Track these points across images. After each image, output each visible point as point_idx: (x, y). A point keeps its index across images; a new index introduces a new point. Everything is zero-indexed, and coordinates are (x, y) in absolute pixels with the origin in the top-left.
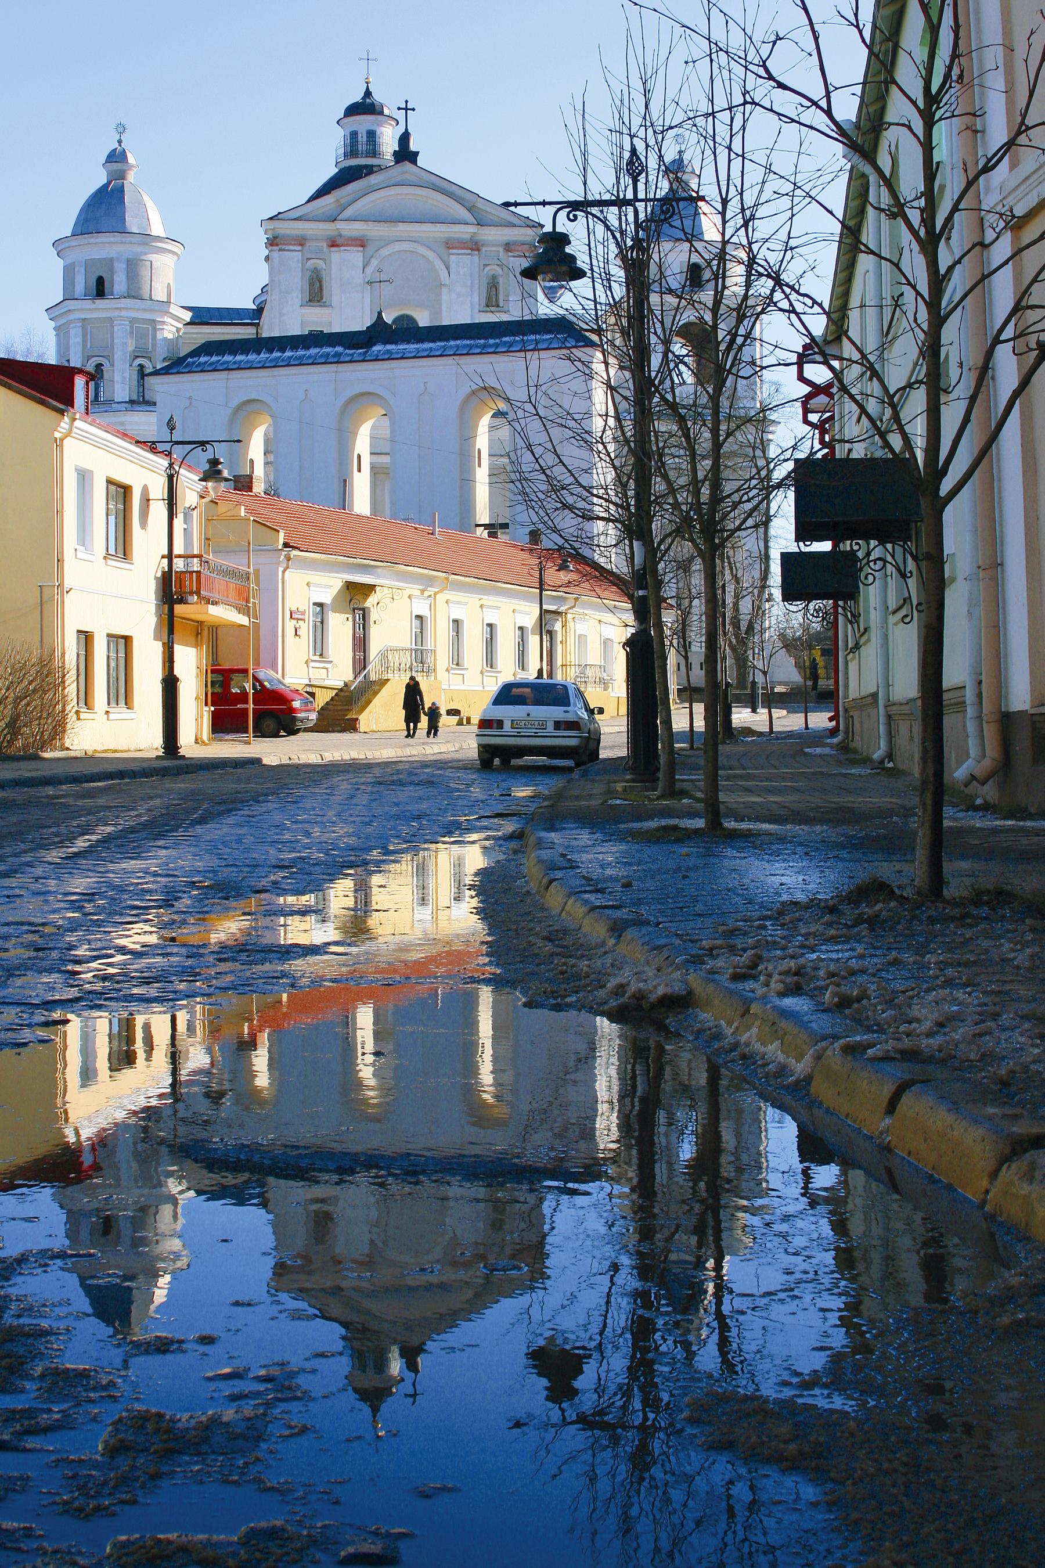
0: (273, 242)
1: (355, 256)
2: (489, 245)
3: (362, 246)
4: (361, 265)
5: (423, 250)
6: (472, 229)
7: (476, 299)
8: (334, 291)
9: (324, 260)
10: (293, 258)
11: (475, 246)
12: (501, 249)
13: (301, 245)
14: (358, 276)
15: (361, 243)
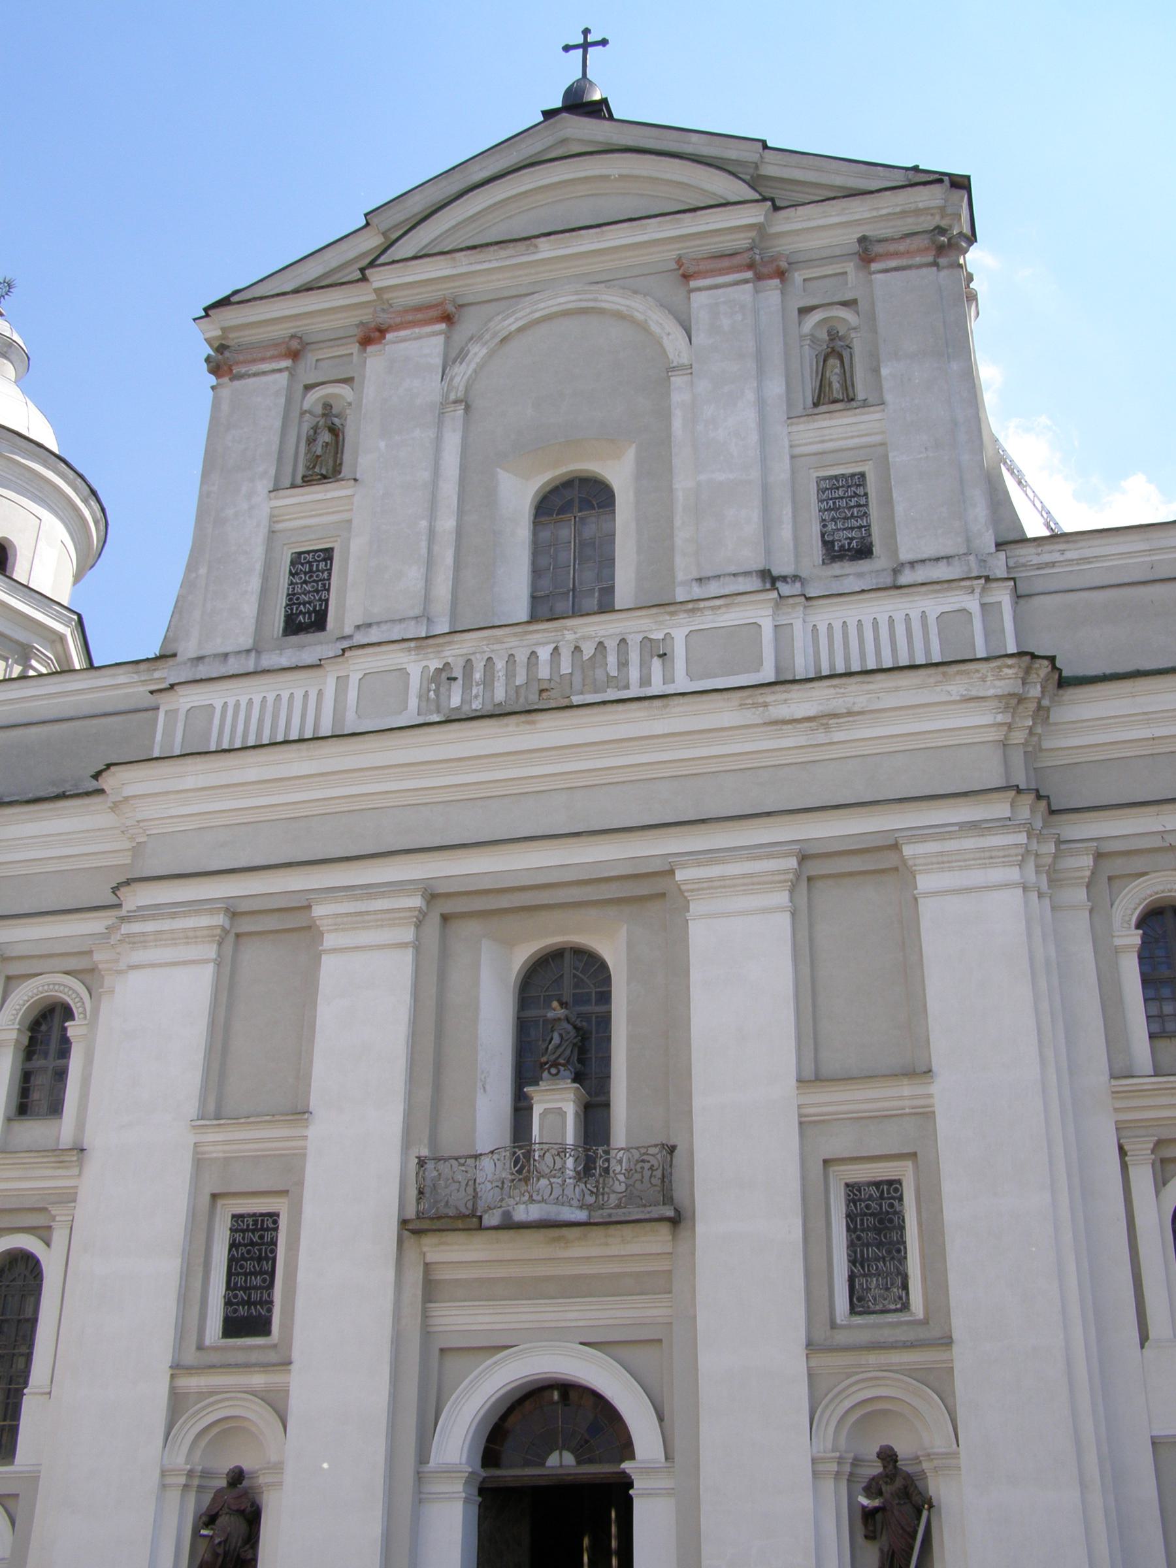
0: (222, 364)
1: (424, 347)
2: (809, 263)
3: (448, 318)
4: (438, 361)
5: (612, 300)
6: (754, 215)
7: (776, 387)
8: (367, 449)
9: (348, 381)
10: (267, 391)
11: (763, 265)
12: (850, 267)
13: (295, 355)
14: (429, 389)
15: (447, 316)
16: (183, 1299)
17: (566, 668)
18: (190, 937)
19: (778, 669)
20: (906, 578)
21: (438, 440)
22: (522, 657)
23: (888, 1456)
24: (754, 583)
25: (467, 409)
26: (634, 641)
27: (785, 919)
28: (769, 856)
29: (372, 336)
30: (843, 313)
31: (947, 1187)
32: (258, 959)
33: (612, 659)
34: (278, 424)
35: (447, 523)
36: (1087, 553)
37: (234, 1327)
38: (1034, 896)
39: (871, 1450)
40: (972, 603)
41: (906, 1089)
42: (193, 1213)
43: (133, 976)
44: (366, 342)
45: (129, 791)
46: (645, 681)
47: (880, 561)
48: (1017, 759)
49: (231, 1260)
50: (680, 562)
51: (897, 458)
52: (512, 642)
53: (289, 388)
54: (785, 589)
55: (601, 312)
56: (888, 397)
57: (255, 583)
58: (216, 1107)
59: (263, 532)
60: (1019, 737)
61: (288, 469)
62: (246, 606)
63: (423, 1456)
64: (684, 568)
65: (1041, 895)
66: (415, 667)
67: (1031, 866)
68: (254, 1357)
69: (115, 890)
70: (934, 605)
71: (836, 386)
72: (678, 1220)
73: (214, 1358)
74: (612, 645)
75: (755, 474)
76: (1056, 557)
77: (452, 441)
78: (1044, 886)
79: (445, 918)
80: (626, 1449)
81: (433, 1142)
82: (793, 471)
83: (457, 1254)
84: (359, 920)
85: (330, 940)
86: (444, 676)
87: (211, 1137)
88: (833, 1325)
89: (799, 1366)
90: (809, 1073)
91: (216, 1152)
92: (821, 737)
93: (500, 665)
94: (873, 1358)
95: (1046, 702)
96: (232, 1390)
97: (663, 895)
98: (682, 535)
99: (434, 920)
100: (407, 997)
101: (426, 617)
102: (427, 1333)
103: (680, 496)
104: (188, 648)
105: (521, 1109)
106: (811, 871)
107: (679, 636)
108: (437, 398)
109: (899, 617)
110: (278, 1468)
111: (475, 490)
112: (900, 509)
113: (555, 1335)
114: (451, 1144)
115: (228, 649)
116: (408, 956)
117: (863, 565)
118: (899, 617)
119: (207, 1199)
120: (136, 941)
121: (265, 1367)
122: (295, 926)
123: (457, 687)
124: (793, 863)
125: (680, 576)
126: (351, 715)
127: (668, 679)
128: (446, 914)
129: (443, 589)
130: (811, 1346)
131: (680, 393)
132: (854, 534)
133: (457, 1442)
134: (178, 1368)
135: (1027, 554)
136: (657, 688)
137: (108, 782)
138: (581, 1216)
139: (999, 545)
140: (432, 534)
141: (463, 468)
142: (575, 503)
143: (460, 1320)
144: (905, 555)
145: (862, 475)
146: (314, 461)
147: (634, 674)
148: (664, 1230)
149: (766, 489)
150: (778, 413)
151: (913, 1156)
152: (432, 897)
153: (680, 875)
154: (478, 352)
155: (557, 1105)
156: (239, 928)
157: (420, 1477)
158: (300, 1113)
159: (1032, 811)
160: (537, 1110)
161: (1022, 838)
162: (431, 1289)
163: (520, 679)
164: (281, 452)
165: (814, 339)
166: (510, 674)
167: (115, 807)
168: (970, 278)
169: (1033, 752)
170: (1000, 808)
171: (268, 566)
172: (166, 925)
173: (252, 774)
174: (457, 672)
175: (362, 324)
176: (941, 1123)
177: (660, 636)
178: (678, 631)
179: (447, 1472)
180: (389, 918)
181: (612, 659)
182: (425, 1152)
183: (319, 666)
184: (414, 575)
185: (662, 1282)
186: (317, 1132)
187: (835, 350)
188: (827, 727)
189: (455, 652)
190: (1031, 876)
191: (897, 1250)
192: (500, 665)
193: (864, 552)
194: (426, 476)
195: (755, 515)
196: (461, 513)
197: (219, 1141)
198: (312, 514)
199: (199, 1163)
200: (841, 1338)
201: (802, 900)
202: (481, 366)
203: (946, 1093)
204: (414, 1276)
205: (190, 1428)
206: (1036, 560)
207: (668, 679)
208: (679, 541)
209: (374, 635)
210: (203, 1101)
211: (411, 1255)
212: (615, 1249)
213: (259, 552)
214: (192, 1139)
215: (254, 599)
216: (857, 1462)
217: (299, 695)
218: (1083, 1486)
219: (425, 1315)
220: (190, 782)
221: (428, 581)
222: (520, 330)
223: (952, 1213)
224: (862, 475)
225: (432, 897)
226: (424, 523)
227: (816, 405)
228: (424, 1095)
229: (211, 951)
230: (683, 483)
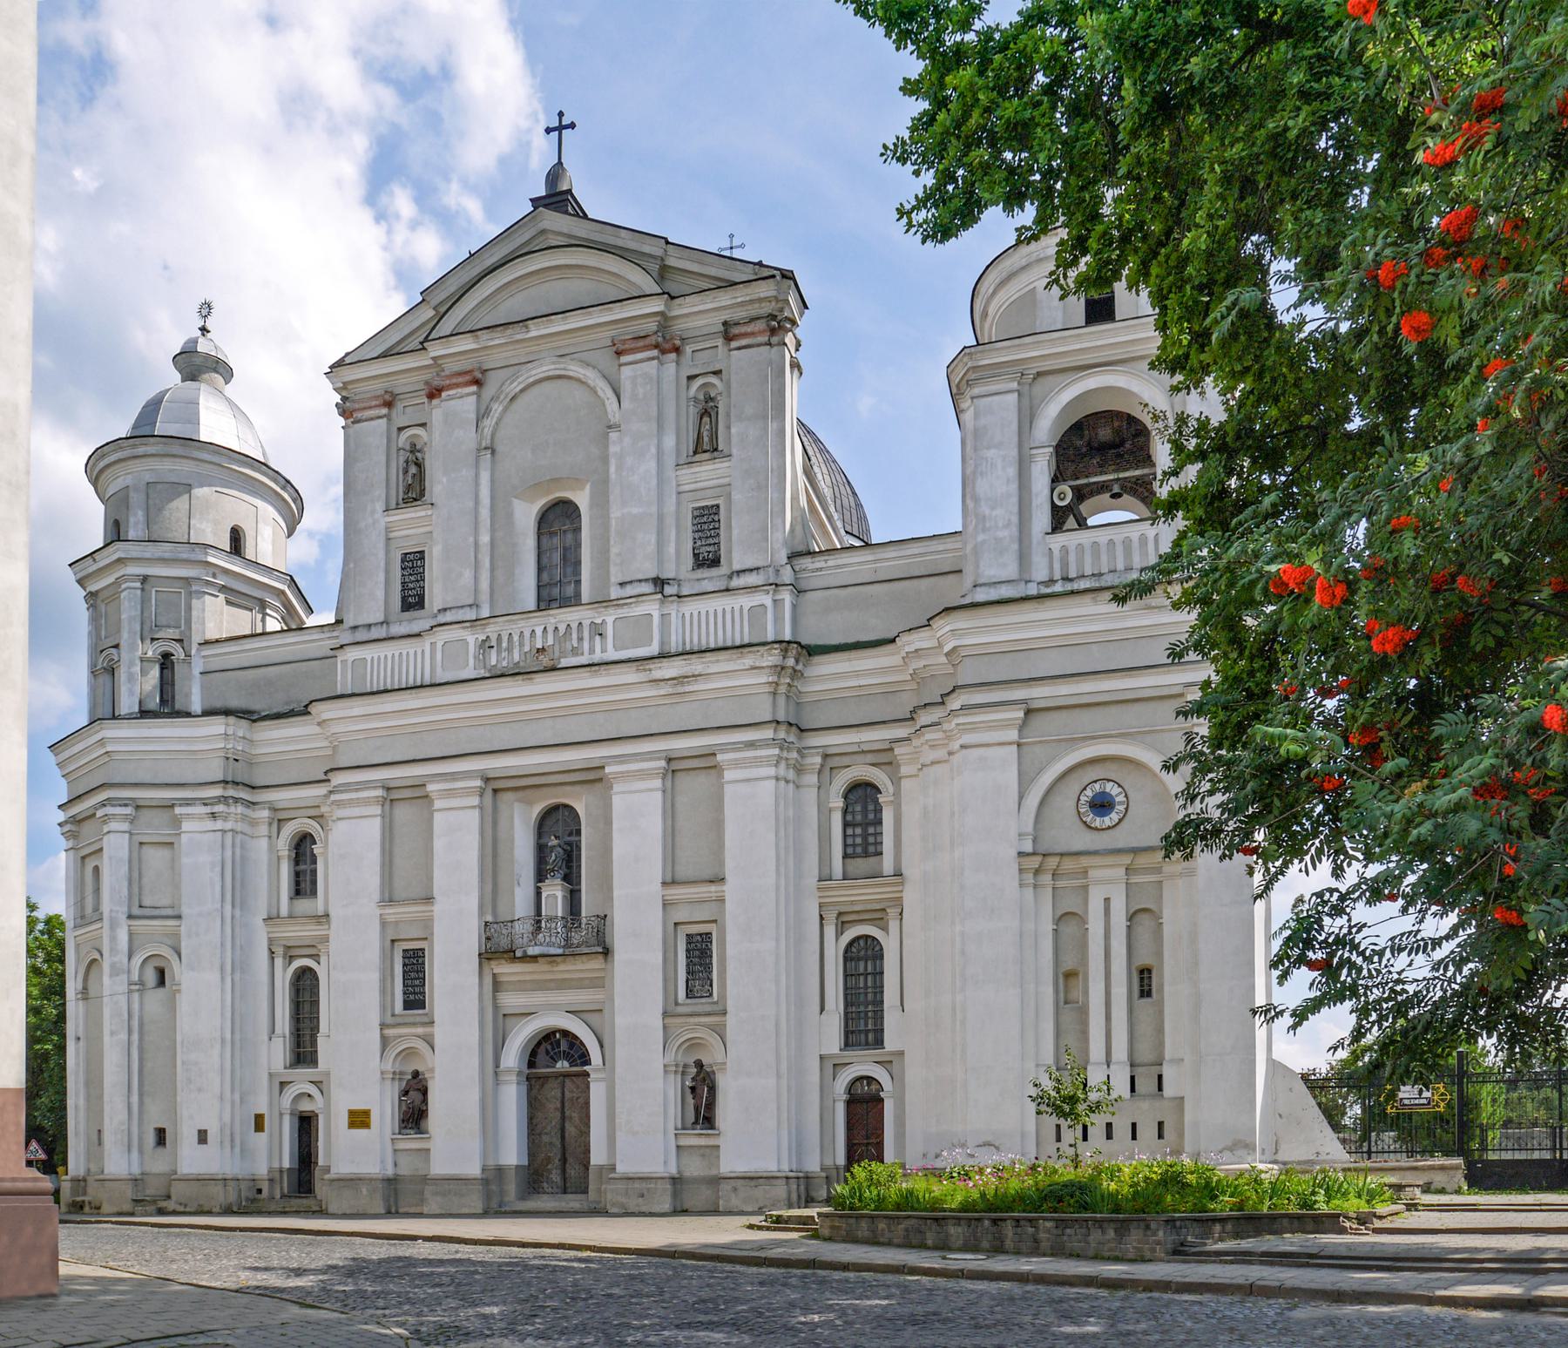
7: (670, 441)
9: (423, 425)
13: (389, 404)
16: (383, 992)
17: (550, 641)
18: (366, 802)
19: (662, 643)
20: (735, 582)
21: (477, 476)
22: (527, 634)
23: (699, 1064)
24: (647, 588)
25: (493, 452)
26: (586, 623)
27: (659, 795)
28: (651, 759)
29: (434, 393)
30: (713, 380)
31: (729, 938)
32: (403, 813)
33: (575, 636)
34: (384, 458)
35: (485, 539)
36: (840, 562)
37: (408, 1005)
38: (782, 783)
39: (691, 1061)
40: (767, 600)
41: (713, 888)
42: (383, 949)
43: (340, 823)
44: (431, 396)
45: (325, 716)
46: (592, 651)
47: (723, 570)
48: (782, 701)
49: (404, 972)
50: (613, 570)
51: (736, 496)
52: (522, 624)
53: (388, 430)
54: (668, 590)
55: (569, 378)
56: (734, 451)
57: (381, 577)
58: (388, 899)
59: (383, 539)
60: (782, 689)
61: (393, 493)
62: (377, 597)
63: (497, 1066)
64: (616, 576)
65: (787, 782)
66: (472, 638)
67: (783, 765)
68: (418, 1019)
69: (326, 773)
70: (747, 601)
71: (706, 439)
72: (607, 952)
73: (399, 1020)
74: (574, 626)
75: (654, 509)
76: (822, 564)
77: (485, 477)
78: (791, 775)
79: (495, 791)
80: (588, 1062)
81: (494, 913)
82: (678, 504)
83: (505, 969)
84: (450, 793)
85: (438, 804)
86: (485, 645)
87: (388, 911)
88: (677, 1004)
89: (657, 1022)
90: (669, 879)
91: (391, 919)
92: (680, 689)
93: (516, 638)
94: (692, 1020)
95: (799, 667)
96: (408, 1036)
97: (600, 780)
98: (614, 550)
99: (489, 793)
100: (477, 836)
101: (475, 605)
102: (496, 1007)
103: (613, 522)
104: (350, 621)
105: (538, 893)
106: (674, 767)
107: (610, 620)
108: (473, 445)
109: (728, 610)
110: (432, 1070)
111: (501, 518)
112: (735, 532)
113: (554, 1007)
114: (504, 915)
115: (371, 621)
116: (476, 813)
117: (714, 572)
118: (728, 610)
119: (388, 943)
120: (339, 804)
121: (424, 1024)
122: (418, 794)
123: (494, 651)
124: (663, 763)
125: (613, 580)
126: (439, 670)
127: (603, 651)
128: (495, 788)
129: (485, 585)
130: (666, 1014)
131: (617, 444)
132: (711, 548)
133: (512, 1057)
134: (383, 1026)
135: (806, 562)
136: (598, 656)
137: (313, 709)
138: (560, 951)
139: (793, 556)
140: (476, 544)
141: (493, 498)
142: (559, 518)
143: (511, 1001)
144: (736, 567)
145: (718, 506)
146: (409, 488)
147: (586, 645)
148: (601, 957)
149: (661, 518)
150: (670, 461)
151: (715, 921)
152: (487, 780)
153: (607, 770)
154: (497, 408)
155: (555, 892)
156: (391, 796)
157: (496, 1073)
158: (429, 899)
159: (788, 733)
160: (544, 895)
161: (777, 751)
162: (497, 986)
163: (527, 649)
164: (388, 480)
165: (695, 399)
166: (521, 645)
167: (319, 724)
168: (798, 345)
169: (794, 697)
170: (768, 733)
171: (387, 564)
172: (353, 795)
173: (388, 707)
174: (494, 643)
175: (427, 383)
176: (728, 905)
177: (598, 621)
178: (609, 617)
179: (509, 1071)
180: (467, 792)
181: (575, 636)
182: (489, 918)
183: (418, 635)
184: (468, 574)
185: (600, 983)
186: (437, 908)
187: (708, 410)
188: (682, 684)
189: (492, 630)
190: (782, 771)
191: (708, 968)
192: (516, 638)
193: (715, 562)
194: (471, 504)
195: (653, 539)
196: (493, 530)
197: (392, 912)
198: (411, 525)
199: (384, 924)
200: (680, 1010)
201: (669, 784)
202: (499, 420)
203: (730, 889)
204: (488, 980)
205: (391, 1054)
206: (811, 566)
207: (603, 651)
208: (612, 556)
209: (448, 617)
210: (382, 892)
211: (487, 970)
212: (580, 967)
213: (381, 554)
214: (378, 912)
215: (382, 586)
216: (685, 1066)
217: (412, 653)
218: (778, 1076)
219: (495, 998)
220: (356, 711)
221: (476, 578)
222: (522, 391)
223: (730, 951)
224: (718, 506)
225: (487, 780)
226: (471, 539)
227: (695, 453)
228: (489, 887)
229: (378, 810)
230: (616, 513)
